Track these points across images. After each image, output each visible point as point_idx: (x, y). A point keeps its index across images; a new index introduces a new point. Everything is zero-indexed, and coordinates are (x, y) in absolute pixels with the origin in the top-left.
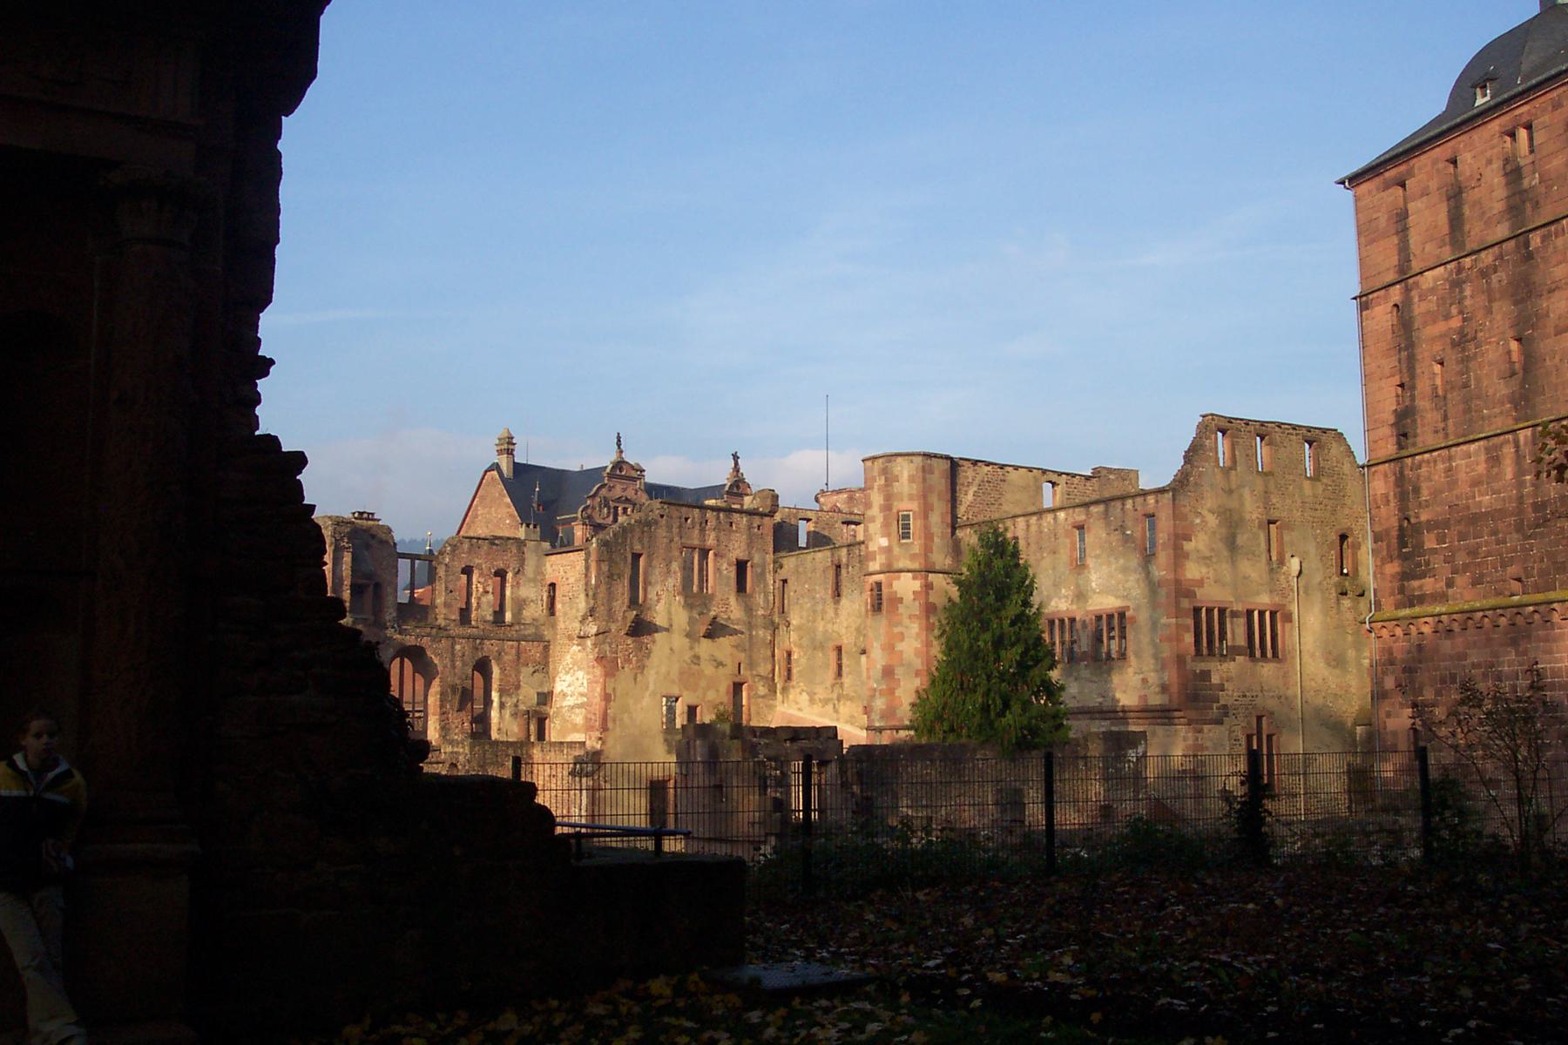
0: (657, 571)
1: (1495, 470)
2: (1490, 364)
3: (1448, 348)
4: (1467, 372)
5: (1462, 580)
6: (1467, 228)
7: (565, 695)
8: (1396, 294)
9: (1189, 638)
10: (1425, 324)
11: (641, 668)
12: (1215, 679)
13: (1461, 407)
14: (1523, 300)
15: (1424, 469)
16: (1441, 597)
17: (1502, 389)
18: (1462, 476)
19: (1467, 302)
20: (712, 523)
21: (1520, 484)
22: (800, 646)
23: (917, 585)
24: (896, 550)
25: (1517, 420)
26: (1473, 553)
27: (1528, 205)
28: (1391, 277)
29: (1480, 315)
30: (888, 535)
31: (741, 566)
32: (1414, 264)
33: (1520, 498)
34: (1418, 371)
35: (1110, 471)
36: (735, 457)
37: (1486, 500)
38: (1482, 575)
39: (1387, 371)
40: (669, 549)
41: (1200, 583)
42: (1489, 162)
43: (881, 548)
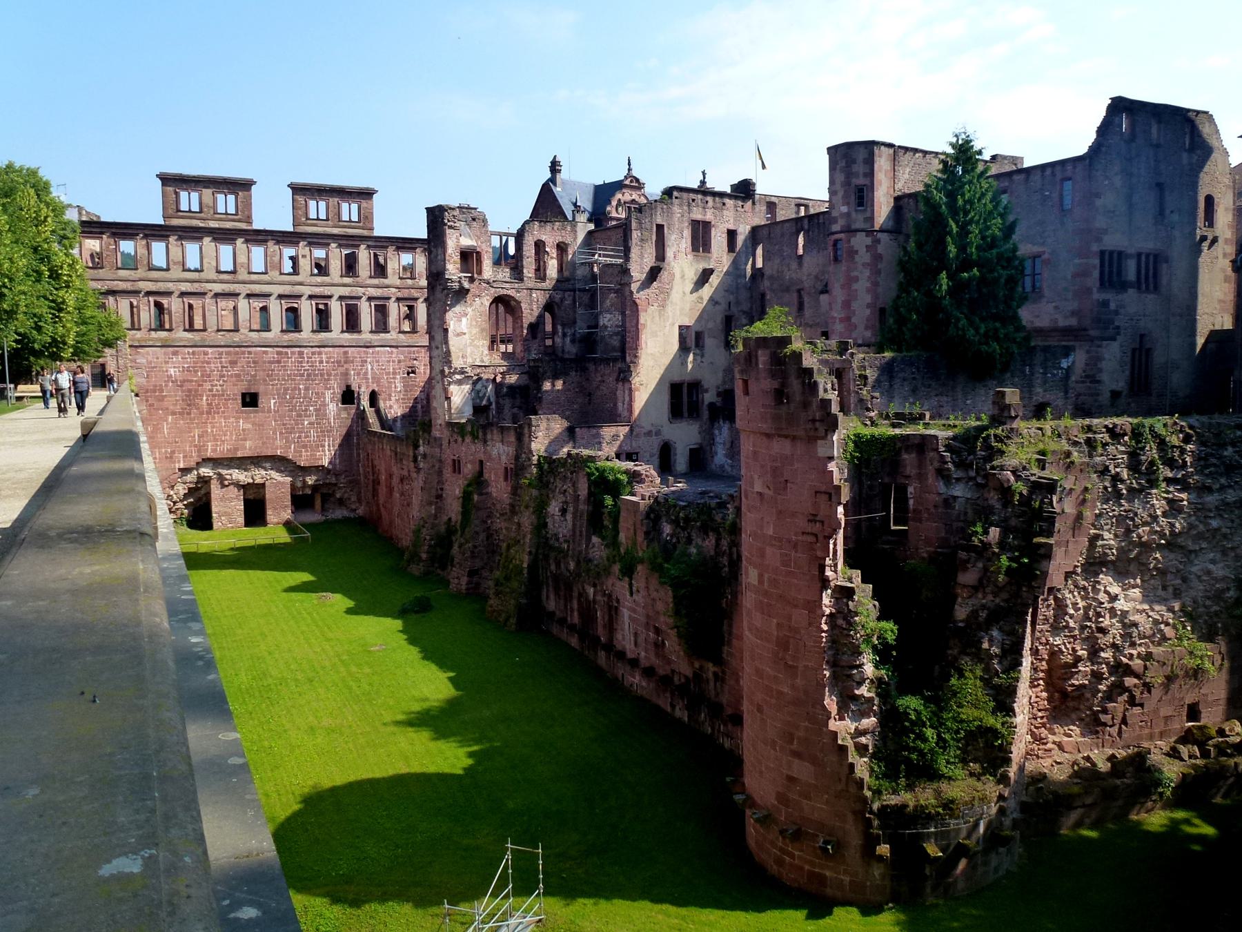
0: (673, 237)
7: (606, 327)
9: (1096, 274)
11: (663, 307)
12: (1113, 306)
20: (710, 204)
22: (773, 291)
23: (869, 241)
24: (854, 215)
30: (848, 204)
31: (732, 234)
35: (1005, 157)
36: (704, 173)
40: (681, 222)
41: (1105, 231)
43: (842, 215)
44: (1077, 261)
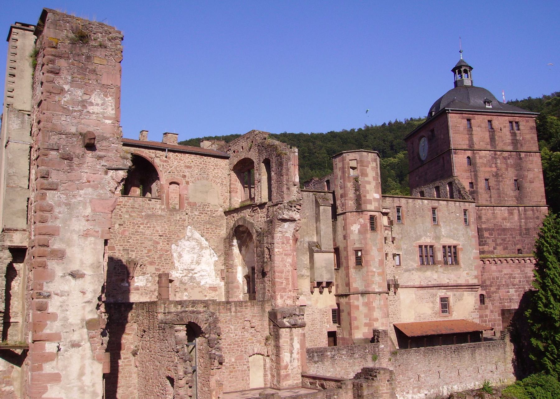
1: (511, 216)
2: (508, 185)
3: (491, 176)
4: (499, 185)
5: (499, 248)
6: (497, 143)
8: (469, 153)
10: (482, 166)
13: (497, 195)
14: (518, 170)
15: (483, 211)
16: (492, 252)
17: (512, 193)
18: (499, 216)
19: (499, 165)
21: (520, 222)
25: (517, 203)
26: (504, 240)
27: (519, 145)
28: (465, 147)
29: (503, 170)
32: (475, 146)
33: (520, 226)
34: (479, 180)
37: (508, 225)
38: (507, 247)
39: (466, 177)
42: (505, 127)
43: (375, 199)
44: (474, 251)
